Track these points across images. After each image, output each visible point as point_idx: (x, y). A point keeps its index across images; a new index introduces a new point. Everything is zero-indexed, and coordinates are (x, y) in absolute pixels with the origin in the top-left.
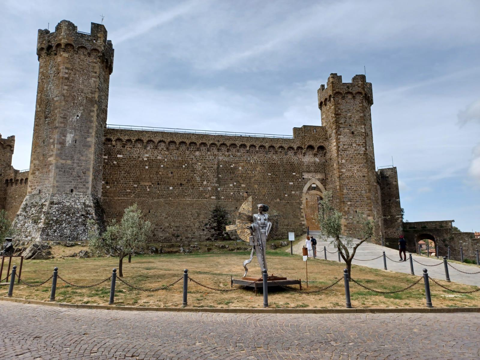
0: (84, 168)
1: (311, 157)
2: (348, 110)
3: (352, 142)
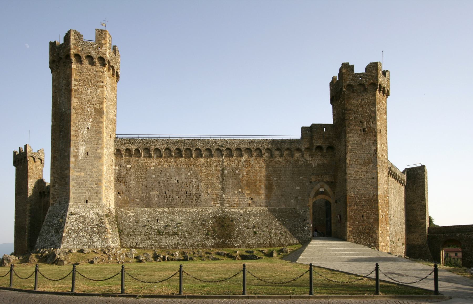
0: (96, 179)
1: (320, 158)
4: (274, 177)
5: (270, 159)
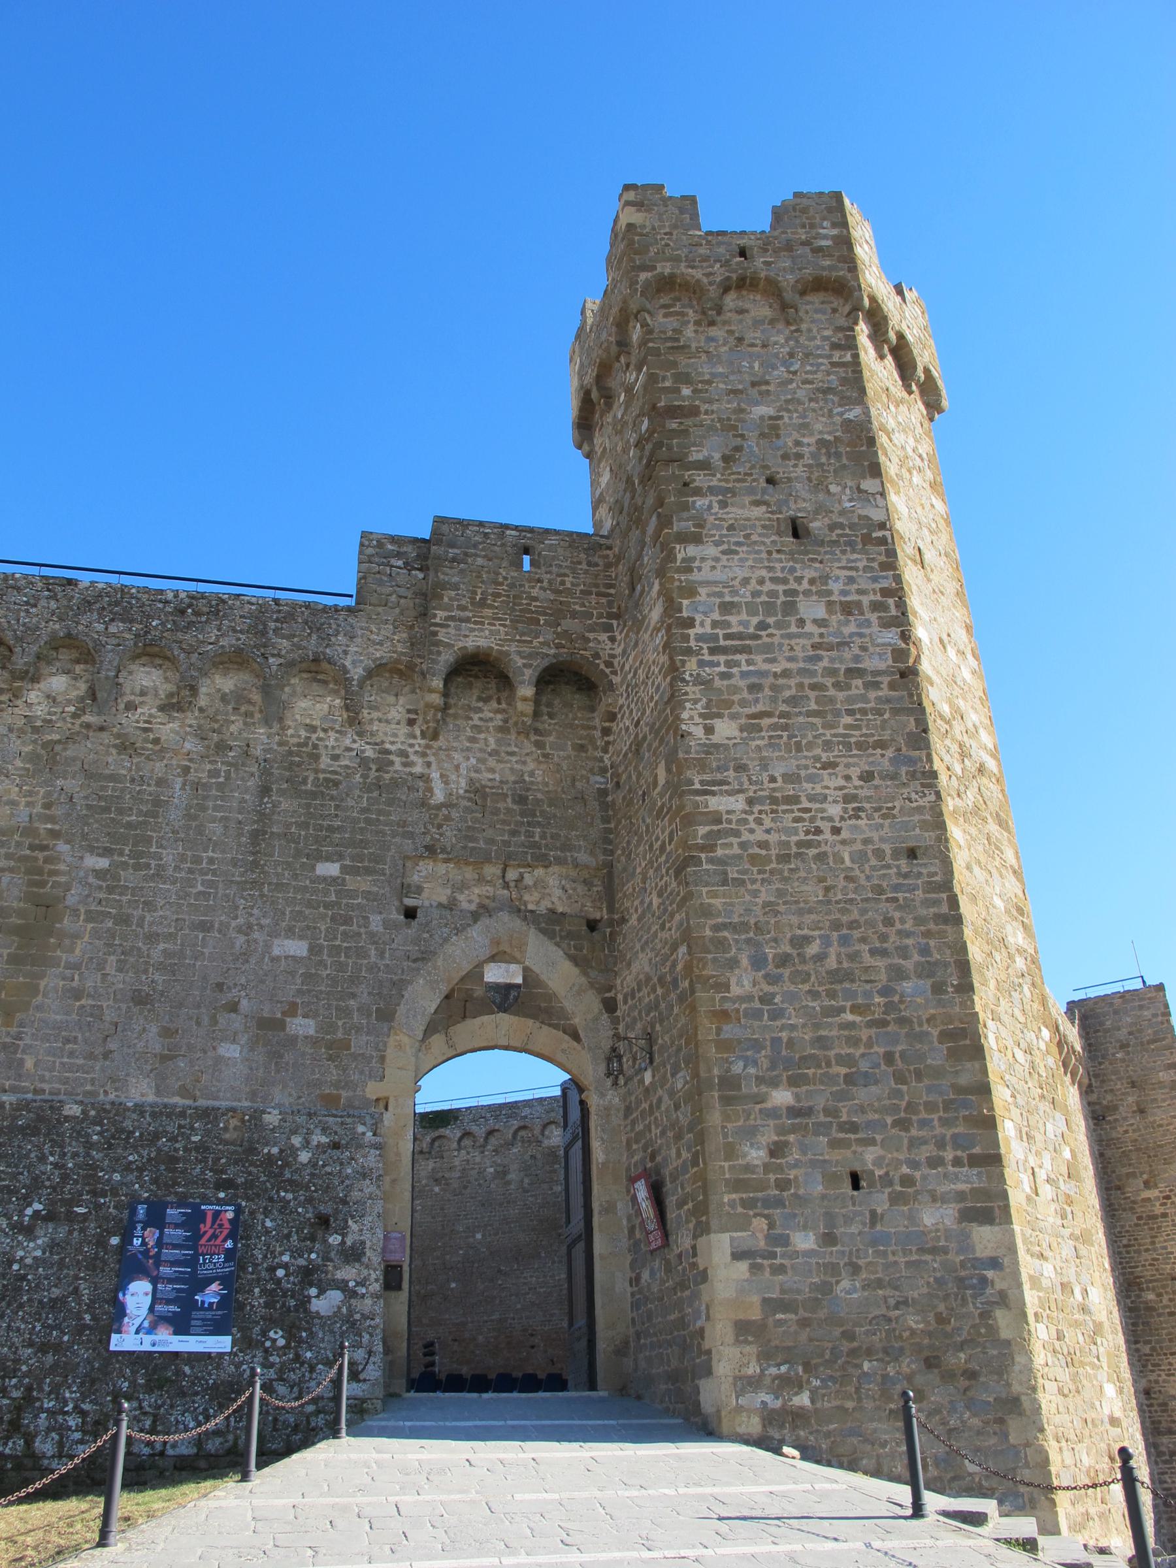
1: (492, 744)
2: (754, 384)
3: (793, 585)
4: (91, 850)
5: (75, 716)
